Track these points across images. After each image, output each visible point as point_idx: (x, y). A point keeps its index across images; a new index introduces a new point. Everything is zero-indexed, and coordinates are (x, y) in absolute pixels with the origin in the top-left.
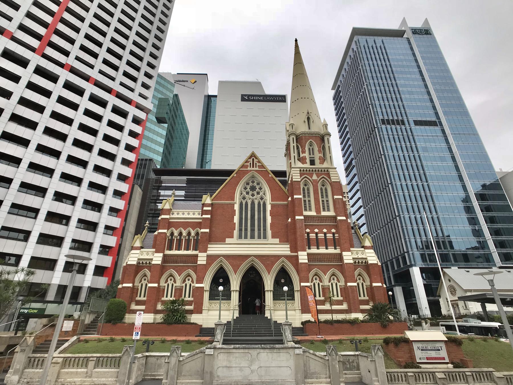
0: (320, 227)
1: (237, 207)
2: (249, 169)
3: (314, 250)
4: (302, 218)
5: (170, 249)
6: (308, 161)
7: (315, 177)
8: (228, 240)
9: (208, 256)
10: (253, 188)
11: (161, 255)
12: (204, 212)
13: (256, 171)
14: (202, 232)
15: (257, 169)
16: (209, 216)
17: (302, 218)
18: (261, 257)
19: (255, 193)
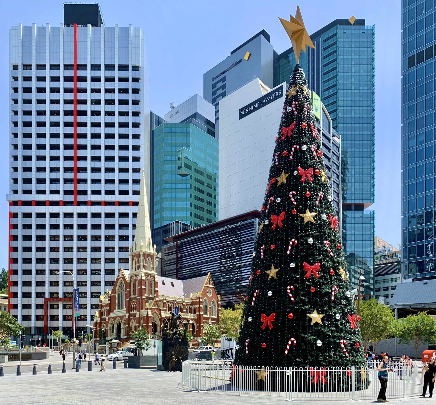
0: (134, 302)
1: (117, 297)
2: (120, 277)
3: (132, 312)
4: (128, 299)
5: (103, 316)
6: (134, 269)
7: (135, 278)
8: (115, 311)
9: (109, 318)
10: (121, 286)
11: (100, 318)
12: (108, 301)
13: (122, 277)
14: (107, 309)
15: (122, 276)
16: (109, 302)
17: (128, 299)
18: (120, 317)
19: (122, 288)
